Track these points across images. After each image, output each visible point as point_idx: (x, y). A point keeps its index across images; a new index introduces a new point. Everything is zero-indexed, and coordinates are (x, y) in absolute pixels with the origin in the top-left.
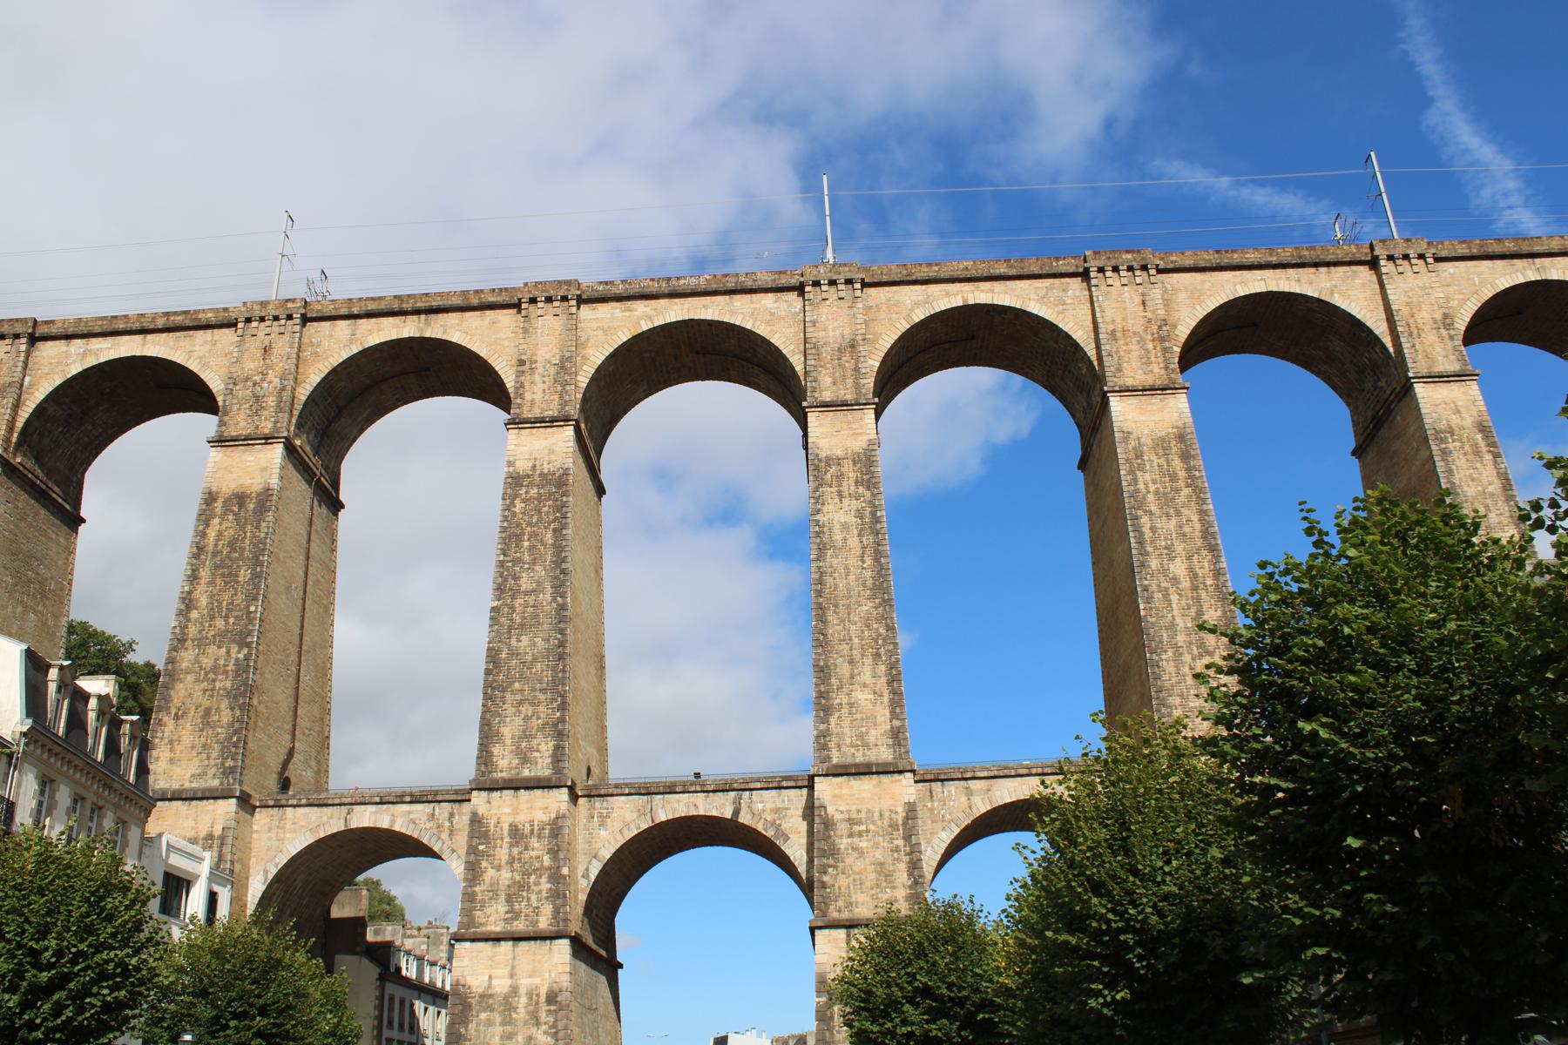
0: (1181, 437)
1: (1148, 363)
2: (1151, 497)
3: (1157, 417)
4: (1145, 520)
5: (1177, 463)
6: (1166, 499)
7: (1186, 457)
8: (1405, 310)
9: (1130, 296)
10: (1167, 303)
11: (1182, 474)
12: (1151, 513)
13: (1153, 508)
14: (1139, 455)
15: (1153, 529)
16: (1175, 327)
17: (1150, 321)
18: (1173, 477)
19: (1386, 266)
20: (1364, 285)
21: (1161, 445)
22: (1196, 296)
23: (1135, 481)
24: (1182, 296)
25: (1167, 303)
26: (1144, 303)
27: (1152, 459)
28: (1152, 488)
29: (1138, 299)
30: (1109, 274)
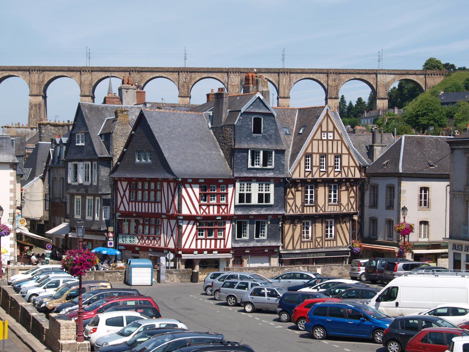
0: (39, 104)
1: (37, 90)
2: (32, 115)
3: (36, 100)
4: (31, 119)
5: (38, 109)
6: (35, 116)
7: (39, 108)
8: (83, 82)
9: (37, 76)
10: (43, 77)
11: (38, 111)
12: (32, 118)
13: (32, 117)
14: (32, 107)
15: (32, 121)
16: (44, 81)
17: (39, 81)
18: (37, 112)
19: (82, 73)
20: (78, 75)
21: (36, 105)
22: (49, 76)
23: (30, 112)
24: (46, 76)
25: (43, 77)
26: (39, 77)
27: (34, 108)
28: (33, 113)
29: (38, 77)
30: (33, 71)
